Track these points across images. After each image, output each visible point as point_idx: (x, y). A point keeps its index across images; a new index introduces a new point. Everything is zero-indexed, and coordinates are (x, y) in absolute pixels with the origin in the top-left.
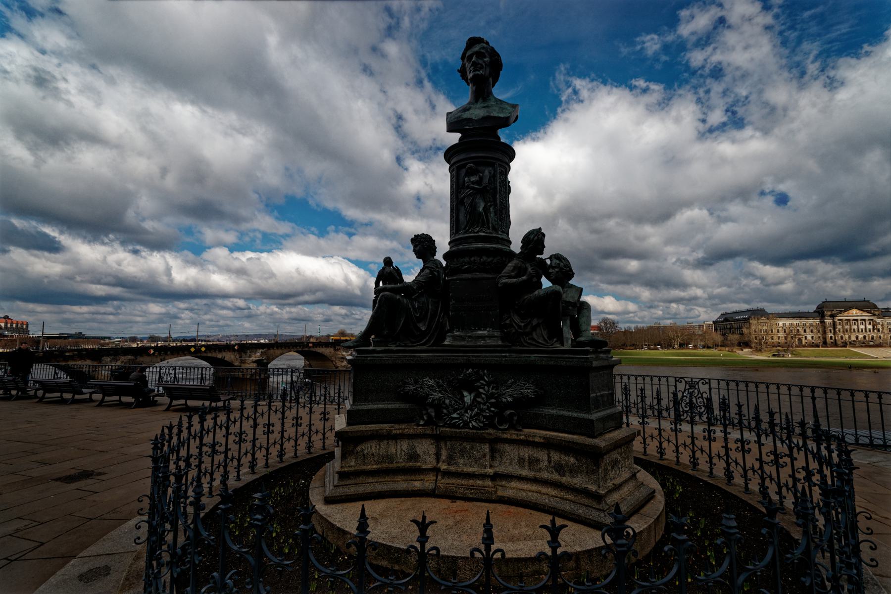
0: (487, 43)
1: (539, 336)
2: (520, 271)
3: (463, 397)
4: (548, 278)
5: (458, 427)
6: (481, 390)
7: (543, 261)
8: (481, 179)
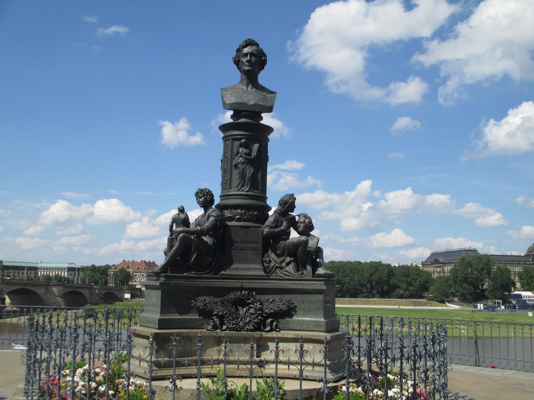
0: (257, 45)
1: (291, 268)
2: (277, 223)
3: (237, 310)
4: (296, 229)
5: (237, 330)
6: (251, 306)
7: (294, 218)
8: (251, 151)
